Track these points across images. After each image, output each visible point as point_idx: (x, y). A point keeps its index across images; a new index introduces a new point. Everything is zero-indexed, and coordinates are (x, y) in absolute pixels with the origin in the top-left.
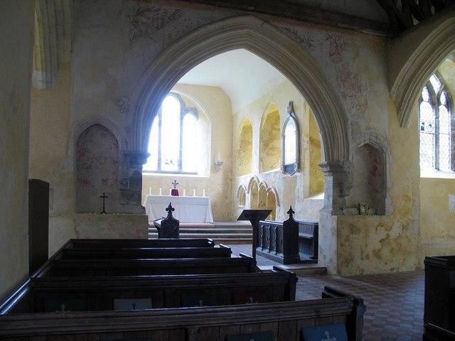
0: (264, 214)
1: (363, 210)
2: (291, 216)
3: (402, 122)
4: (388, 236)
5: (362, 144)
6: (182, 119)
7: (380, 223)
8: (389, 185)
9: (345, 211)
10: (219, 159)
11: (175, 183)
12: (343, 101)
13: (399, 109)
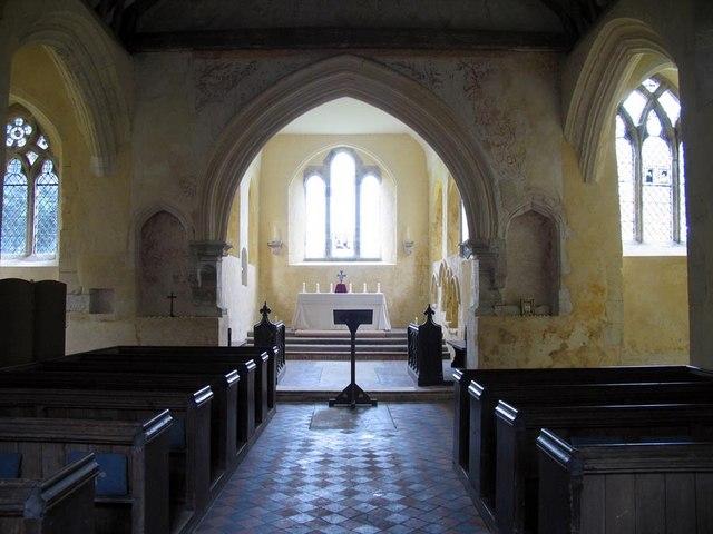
0: (366, 316)
1: (527, 308)
2: (430, 318)
3: (587, 176)
4: (564, 347)
6: (358, 183)
8: (565, 270)
9: (497, 310)
10: (409, 237)
11: (342, 275)
12: (485, 153)
13: (579, 157)
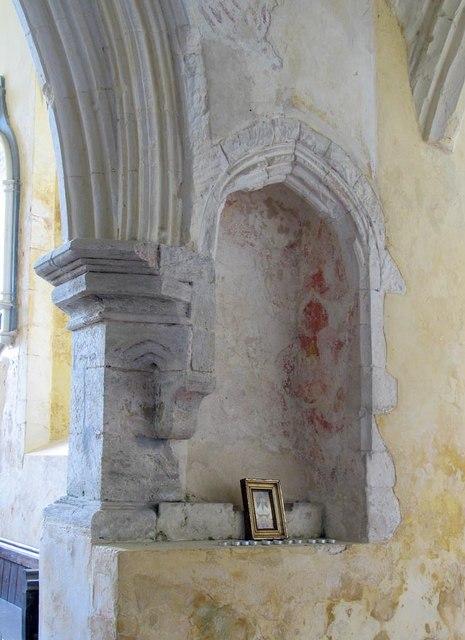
1: (262, 512)
5: (255, 180)
7: (346, 582)
8: (382, 394)
9: (171, 518)
13: (417, 56)
